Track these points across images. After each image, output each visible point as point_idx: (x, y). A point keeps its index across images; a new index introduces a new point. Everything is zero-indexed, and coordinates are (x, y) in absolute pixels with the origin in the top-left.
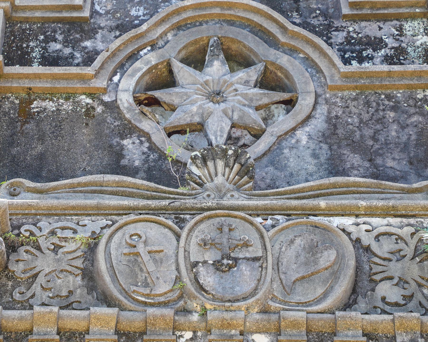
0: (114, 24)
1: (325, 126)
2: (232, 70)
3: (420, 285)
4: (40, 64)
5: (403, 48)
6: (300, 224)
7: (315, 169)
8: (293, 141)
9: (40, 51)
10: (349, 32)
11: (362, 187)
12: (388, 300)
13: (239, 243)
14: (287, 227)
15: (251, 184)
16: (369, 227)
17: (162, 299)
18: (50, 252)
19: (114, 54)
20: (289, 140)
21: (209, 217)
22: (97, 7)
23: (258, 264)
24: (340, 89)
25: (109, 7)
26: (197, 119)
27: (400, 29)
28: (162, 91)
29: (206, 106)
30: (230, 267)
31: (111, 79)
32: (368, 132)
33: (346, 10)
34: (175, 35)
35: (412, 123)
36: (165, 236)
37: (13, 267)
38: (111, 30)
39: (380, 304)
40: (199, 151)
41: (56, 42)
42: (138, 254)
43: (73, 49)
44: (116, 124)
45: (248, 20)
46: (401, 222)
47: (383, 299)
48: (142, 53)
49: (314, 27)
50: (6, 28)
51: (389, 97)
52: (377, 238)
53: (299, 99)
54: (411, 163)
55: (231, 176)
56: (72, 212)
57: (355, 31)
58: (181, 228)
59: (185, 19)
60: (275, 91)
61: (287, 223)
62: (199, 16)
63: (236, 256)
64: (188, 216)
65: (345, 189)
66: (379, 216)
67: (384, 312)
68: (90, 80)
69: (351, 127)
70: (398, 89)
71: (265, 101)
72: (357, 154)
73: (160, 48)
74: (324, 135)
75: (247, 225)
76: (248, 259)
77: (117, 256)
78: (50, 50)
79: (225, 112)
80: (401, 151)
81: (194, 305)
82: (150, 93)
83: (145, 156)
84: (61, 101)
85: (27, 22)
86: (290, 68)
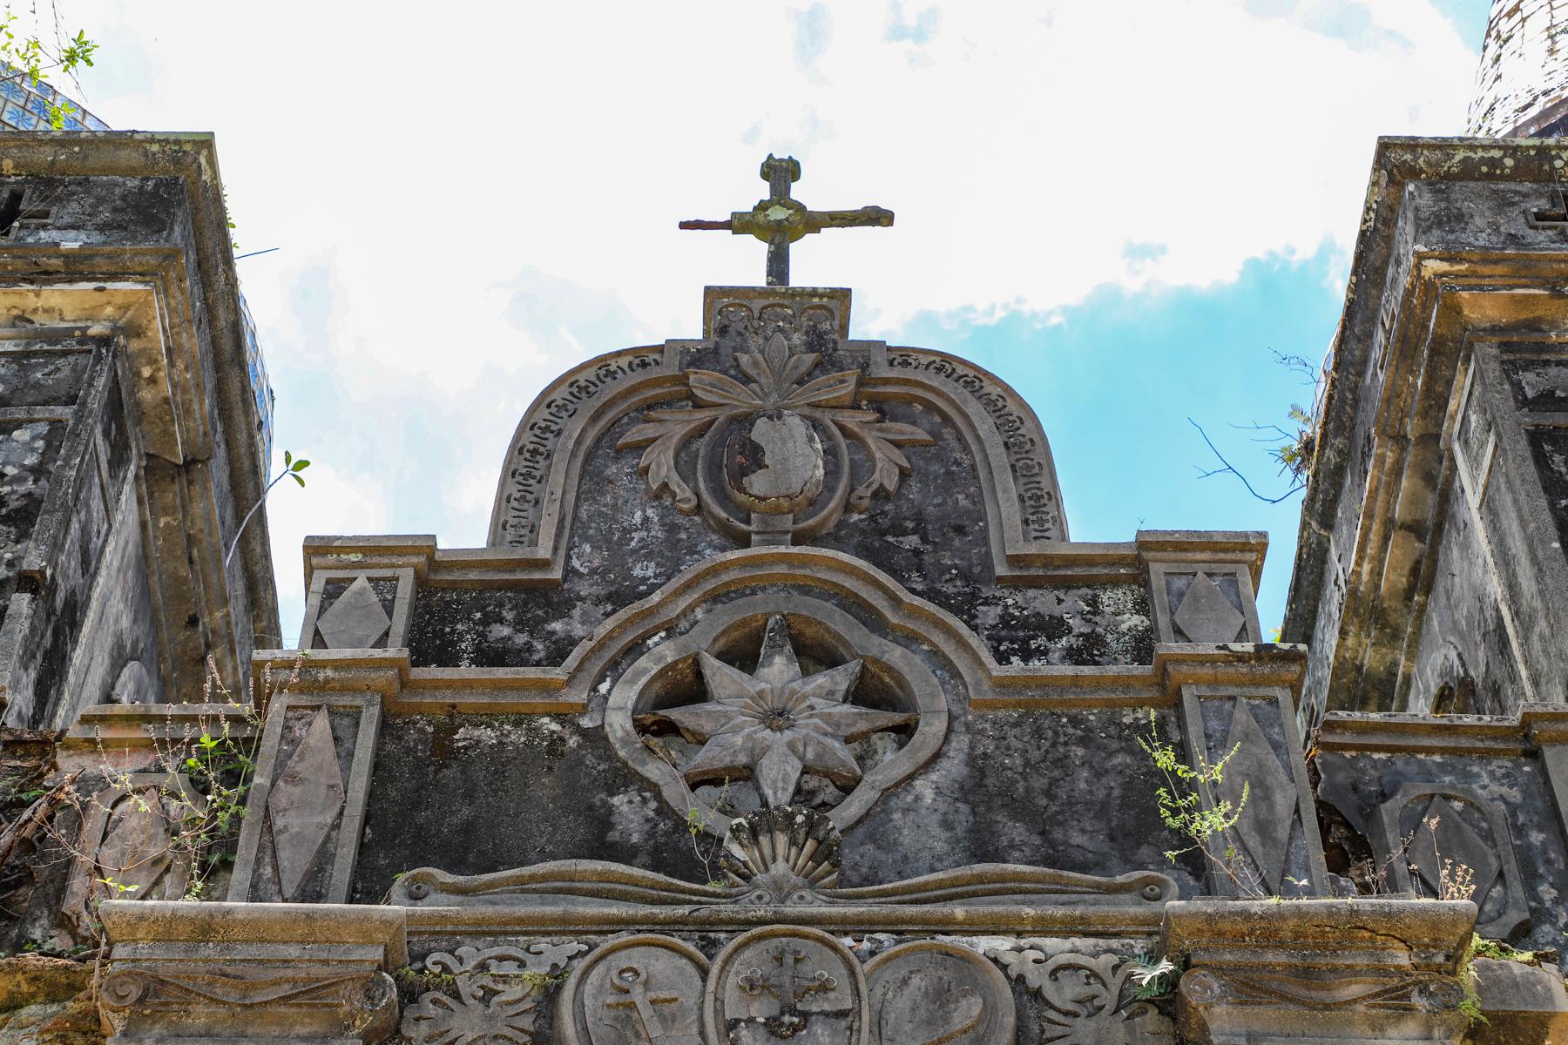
0: (602, 591)
1: (965, 771)
2: (806, 672)
4: (474, 662)
6: (920, 949)
7: (946, 848)
8: (910, 798)
9: (473, 640)
10: (1006, 607)
11: (1028, 881)
13: (811, 984)
14: (896, 956)
15: (835, 876)
16: (1039, 955)
18: (477, 1002)
19: (602, 645)
20: (902, 796)
21: (761, 938)
22: (576, 563)
23: (844, 1024)
24: (992, 706)
25: (596, 563)
26: (742, 759)
27: (1094, 602)
28: (683, 709)
29: (759, 735)
30: (795, 1029)
31: (595, 689)
32: (1039, 783)
33: (1001, 570)
34: (709, 611)
36: (682, 972)
37: (409, 1031)
38: (598, 601)
40: (746, 818)
41: (502, 623)
42: (632, 1006)
43: (531, 634)
44: (601, 768)
45: (835, 585)
46: (1096, 945)
48: (649, 642)
49: (948, 597)
50: (418, 599)
51: (1075, 721)
52: (1054, 974)
53: (921, 723)
54: (1112, 838)
55: (800, 862)
56: (517, 928)
57: (1016, 606)
58: (711, 957)
59: (727, 584)
60: (879, 708)
61: (898, 948)
62: (751, 578)
63: (807, 1008)
64: (722, 936)
65: (998, 885)
66: (1056, 934)
68: (558, 690)
69: (1009, 773)
70: (1090, 707)
71: (862, 726)
72: (1019, 821)
73: (681, 634)
74: (962, 788)
75: (827, 951)
76: (826, 1014)
77: (594, 1010)
78: (491, 638)
79: (791, 746)
80: (1095, 817)
82: (662, 712)
83: (650, 825)
84: (507, 727)
85: (454, 589)
86: (905, 671)
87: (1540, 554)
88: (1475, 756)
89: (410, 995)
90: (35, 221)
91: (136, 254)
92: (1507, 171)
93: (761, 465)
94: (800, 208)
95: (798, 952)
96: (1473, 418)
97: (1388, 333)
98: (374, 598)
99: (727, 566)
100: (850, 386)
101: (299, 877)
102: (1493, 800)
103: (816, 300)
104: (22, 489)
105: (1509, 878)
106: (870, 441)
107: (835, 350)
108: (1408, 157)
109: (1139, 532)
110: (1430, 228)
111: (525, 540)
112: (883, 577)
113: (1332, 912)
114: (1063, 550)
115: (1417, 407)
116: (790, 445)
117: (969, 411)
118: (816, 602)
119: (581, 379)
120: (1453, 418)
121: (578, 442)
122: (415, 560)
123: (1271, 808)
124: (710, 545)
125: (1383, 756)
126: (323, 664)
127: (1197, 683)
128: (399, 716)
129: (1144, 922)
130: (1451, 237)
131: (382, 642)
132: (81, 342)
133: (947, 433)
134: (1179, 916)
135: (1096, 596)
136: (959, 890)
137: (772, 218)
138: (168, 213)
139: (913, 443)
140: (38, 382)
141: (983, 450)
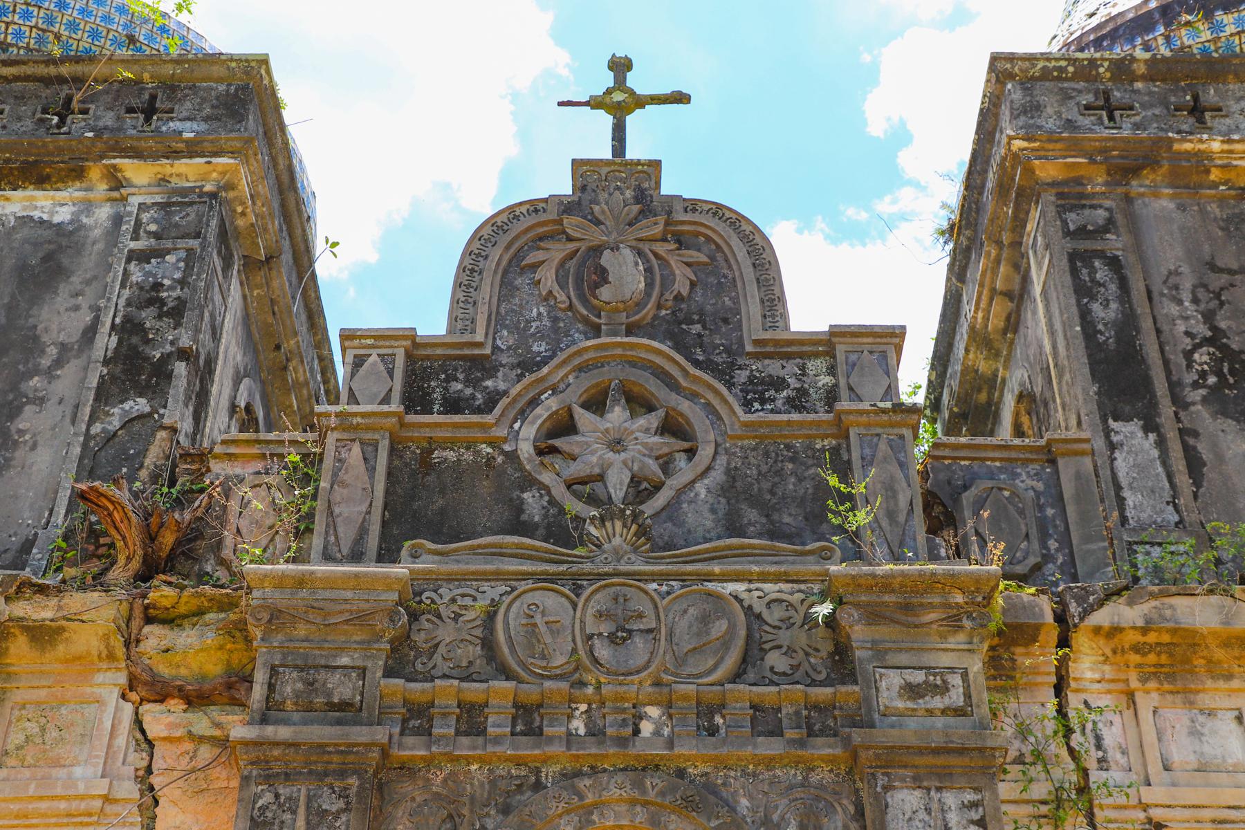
0: (514, 361)
1: (724, 478)
2: (633, 415)
3: (807, 654)
5: (805, 389)
7: (712, 525)
8: (692, 495)
10: (752, 371)
11: (756, 549)
12: (776, 670)
14: (681, 595)
15: (648, 546)
16: (761, 594)
17: (558, 671)
19: (514, 400)
22: (499, 343)
23: (651, 636)
24: (740, 438)
26: (597, 470)
27: (803, 368)
28: (562, 439)
29: (606, 456)
30: (624, 639)
31: (511, 427)
32: (766, 485)
33: (749, 348)
35: (809, 476)
37: (414, 637)
38: (513, 367)
39: (768, 674)
42: (535, 625)
44: (516, 475)
45: (650, 361)
47: (772, 668)
48: (543, 397)
49: (718, 365)
52: (768, 605)
54: (806, 519)
55: (629, 537)
57: (757, 370)
58: (578, 595)
59: (587, 361)
61: (682, 591)
62: (601, 357)
64: (585, 583)
65: (739, 551)
66: (771, 581)
67: (772, 683)
69: (750, 479)
70: (797, 437)
71: (666, 450)
73: (561, 392)
74: (722, 488)
76: (641, 631)
79: (625, 463)
81: (589, 678)
82: (550, 442)
85: (428, 360)
87: (1068, 334)
88: (1019, 463)
89: (414, 616)
90: (166, 115)
91: (228, 140)
92: (1070, 75)
93: (607, 282)
94: (632, 92)
95: (626, 595)
96: (1039, 239)
97: (994, 173)
98: (382, 368)
99: (586, 349)
100: (660, 227)
101: (349, 543)
102: (1026, 490)
103: (640, 167)
104: (174, 294)
105: (1031, 537)
106: (672, 263)
107: (652, 202)
108: (1008, 66)
109: (831, 326)
110: (1019, 115)
111: (468, 328)
112: (678, 357)
113: (921, 574)
114: (785, 336)
115: (1009, 226)
116: (624, 268)
117: (732, 243)
118: (640, 372)
119: (499, 220)
120: (1029, 235)
121: (498, 264)
122: (404, 343)
123: (896, 504)
124: (578, 330)
125: (967, 463)
126: (355, 415)
127: (858, 425)
128: (400, 443)
129: (819, 575)
130: (1031, 122)
131: (386, 400)
132: (200, 197)
133: (719, 256)
134: (836, 577)
135: (804, 364)
136: (718, 554)
137: (615, 100)
138: (245, 109)
139: (698, 263)
140: (177, 223)
141: (740, 269)
